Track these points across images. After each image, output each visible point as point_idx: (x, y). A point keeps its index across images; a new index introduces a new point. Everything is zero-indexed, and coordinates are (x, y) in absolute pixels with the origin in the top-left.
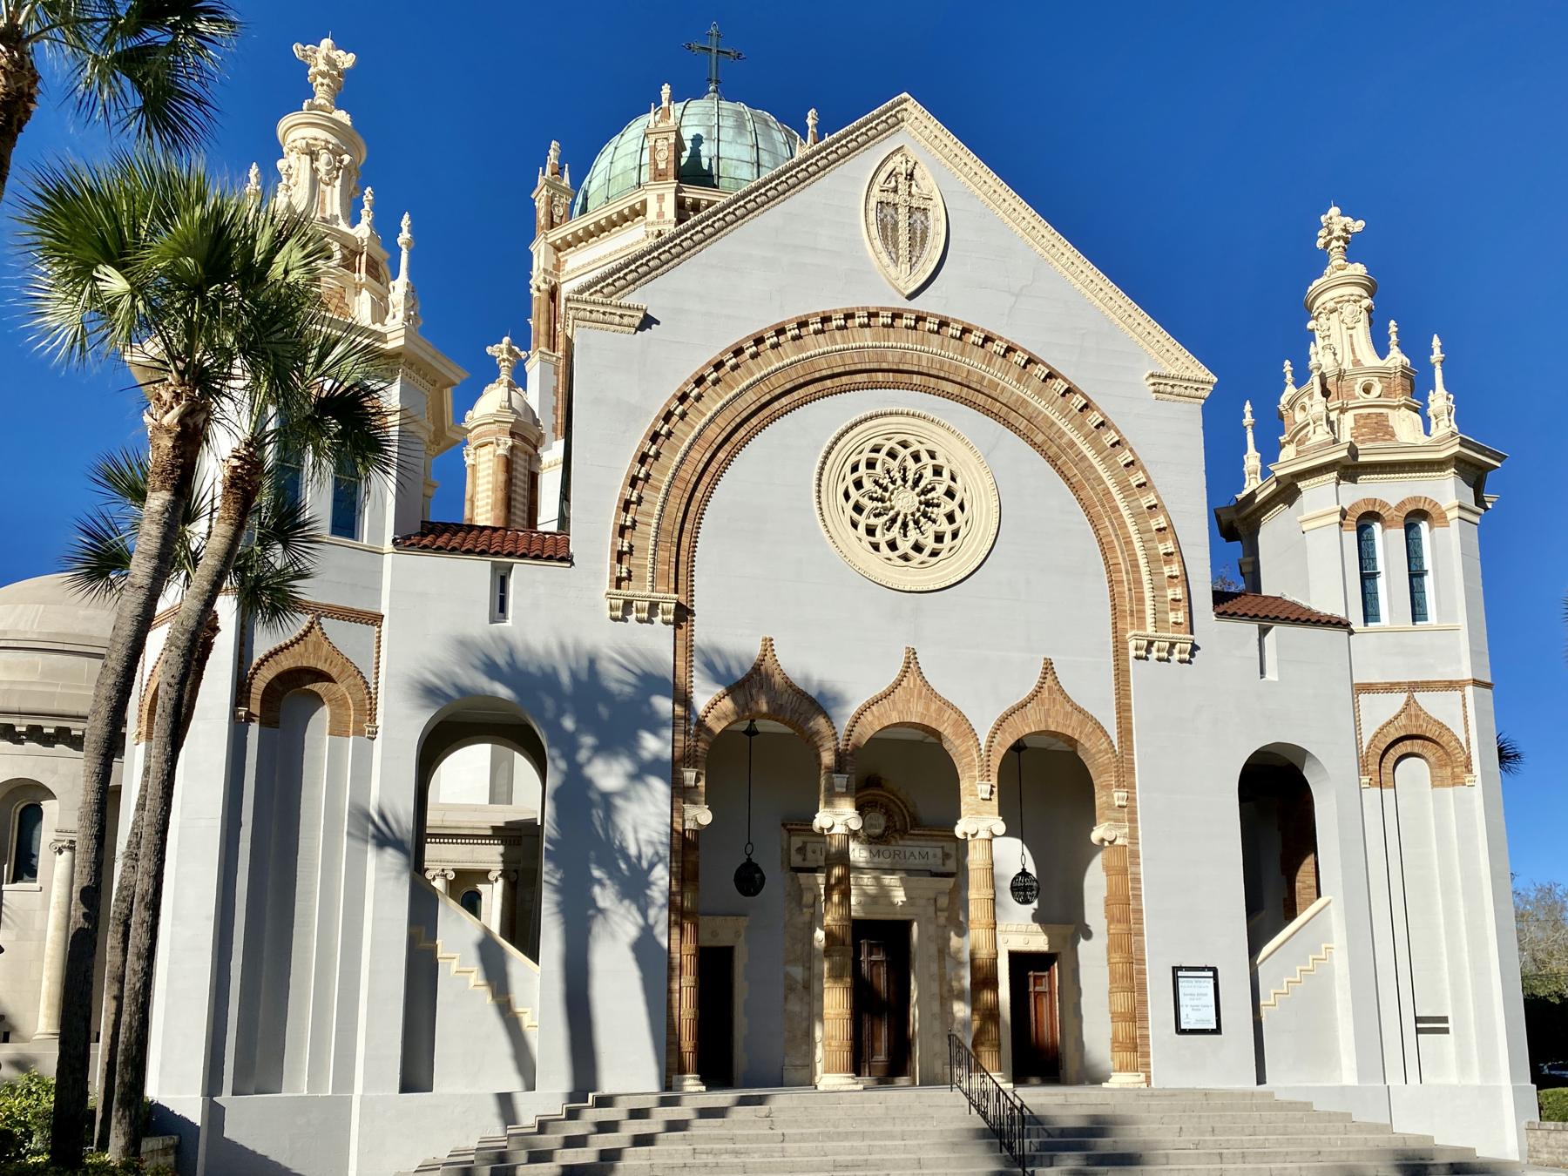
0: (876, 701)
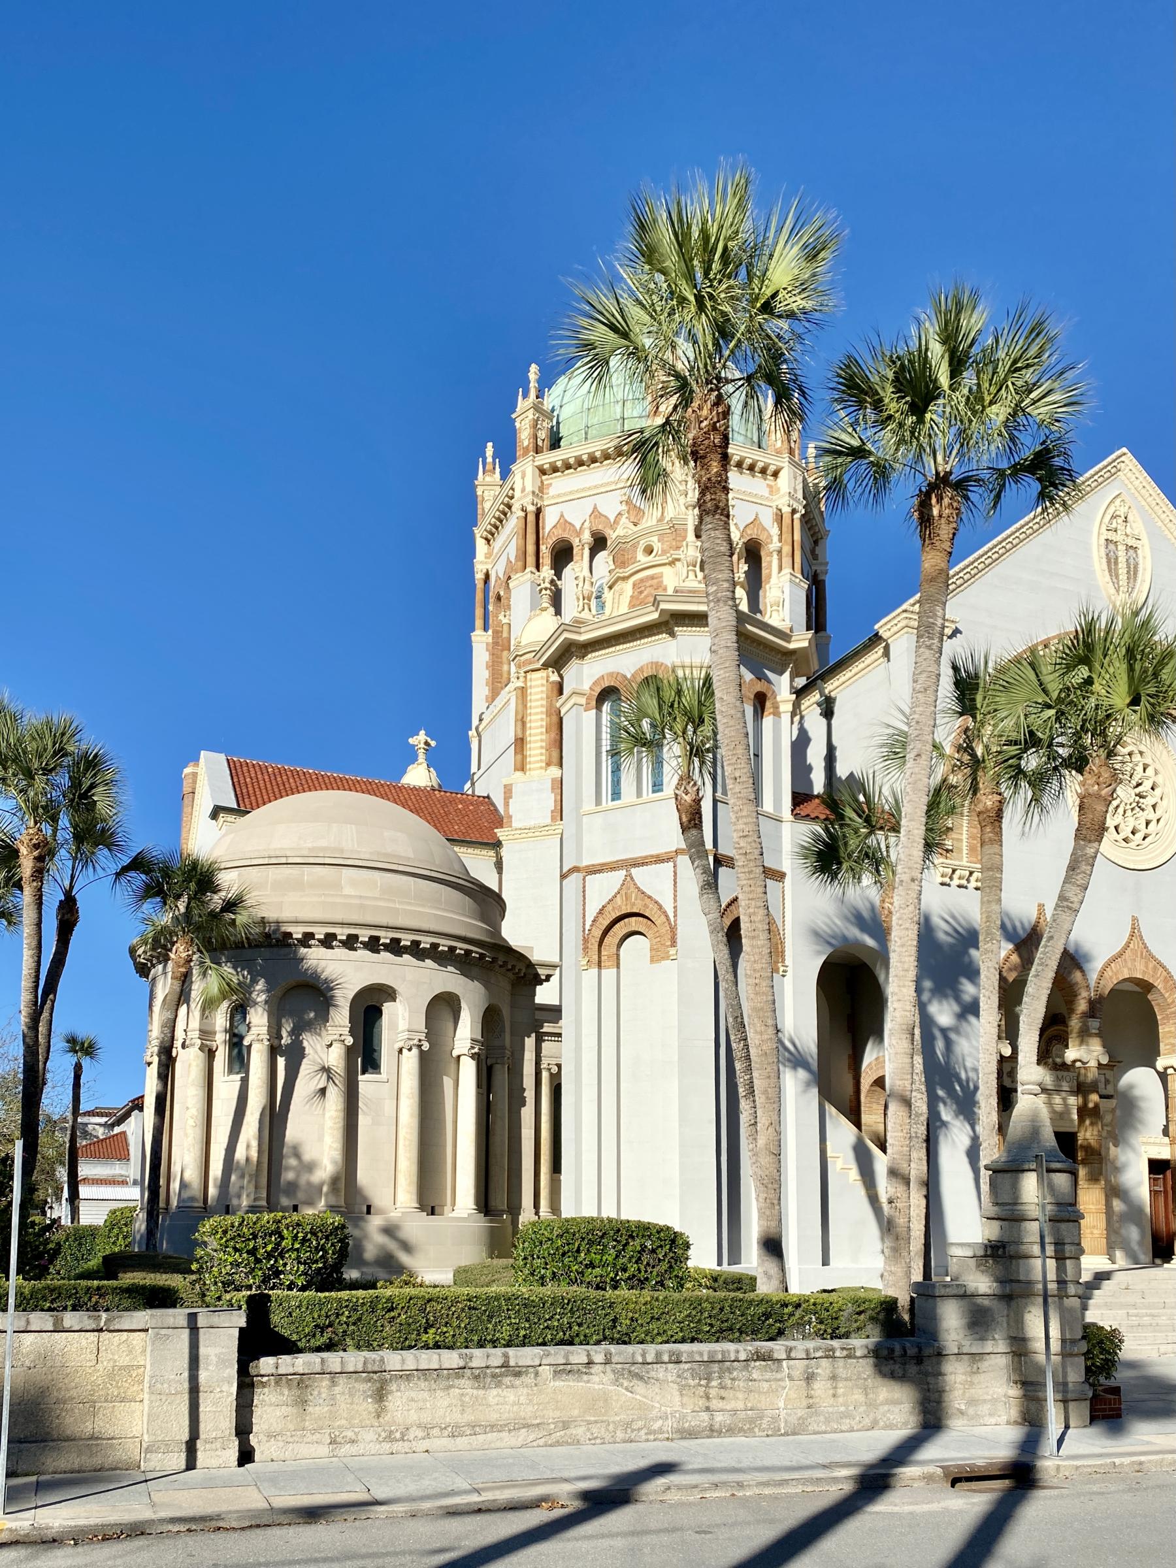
0: (1114, 959)
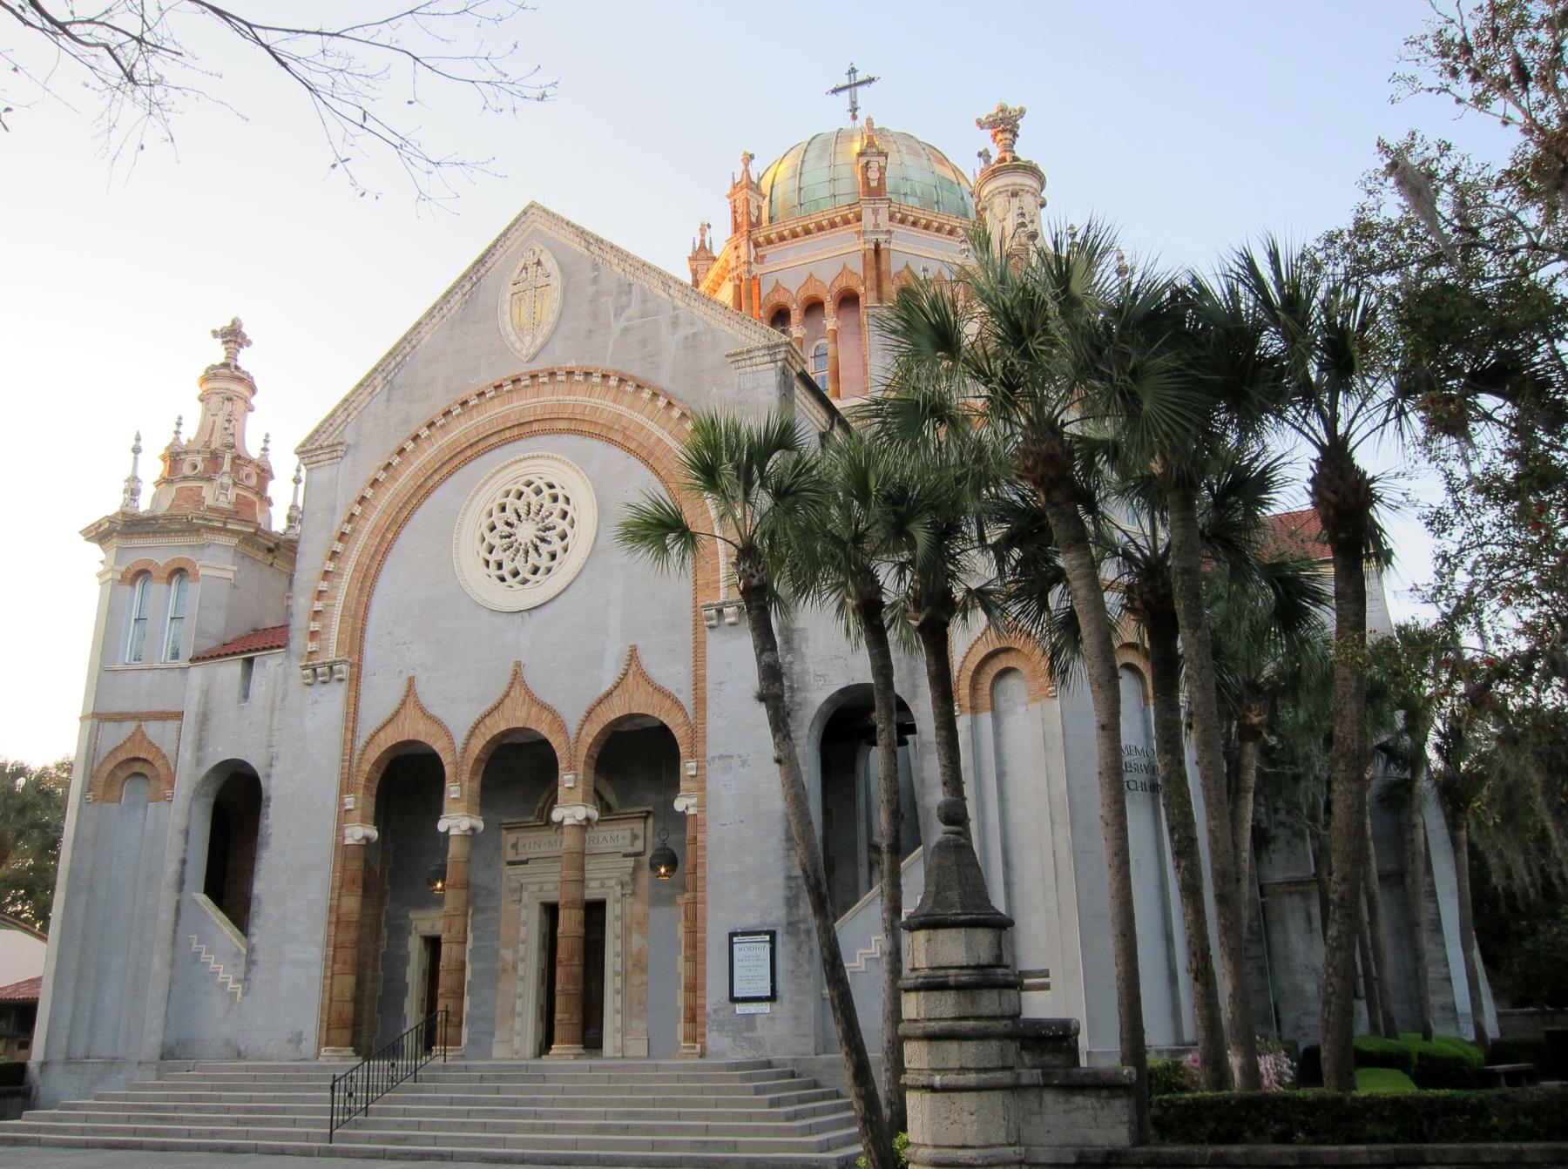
0: (489, 714)
